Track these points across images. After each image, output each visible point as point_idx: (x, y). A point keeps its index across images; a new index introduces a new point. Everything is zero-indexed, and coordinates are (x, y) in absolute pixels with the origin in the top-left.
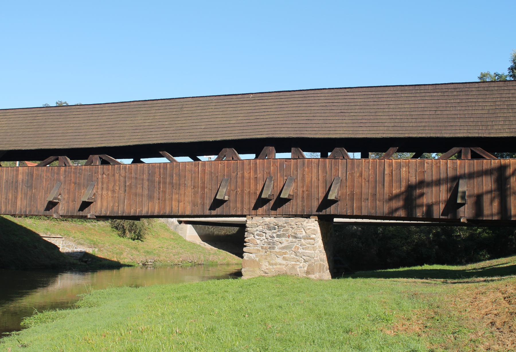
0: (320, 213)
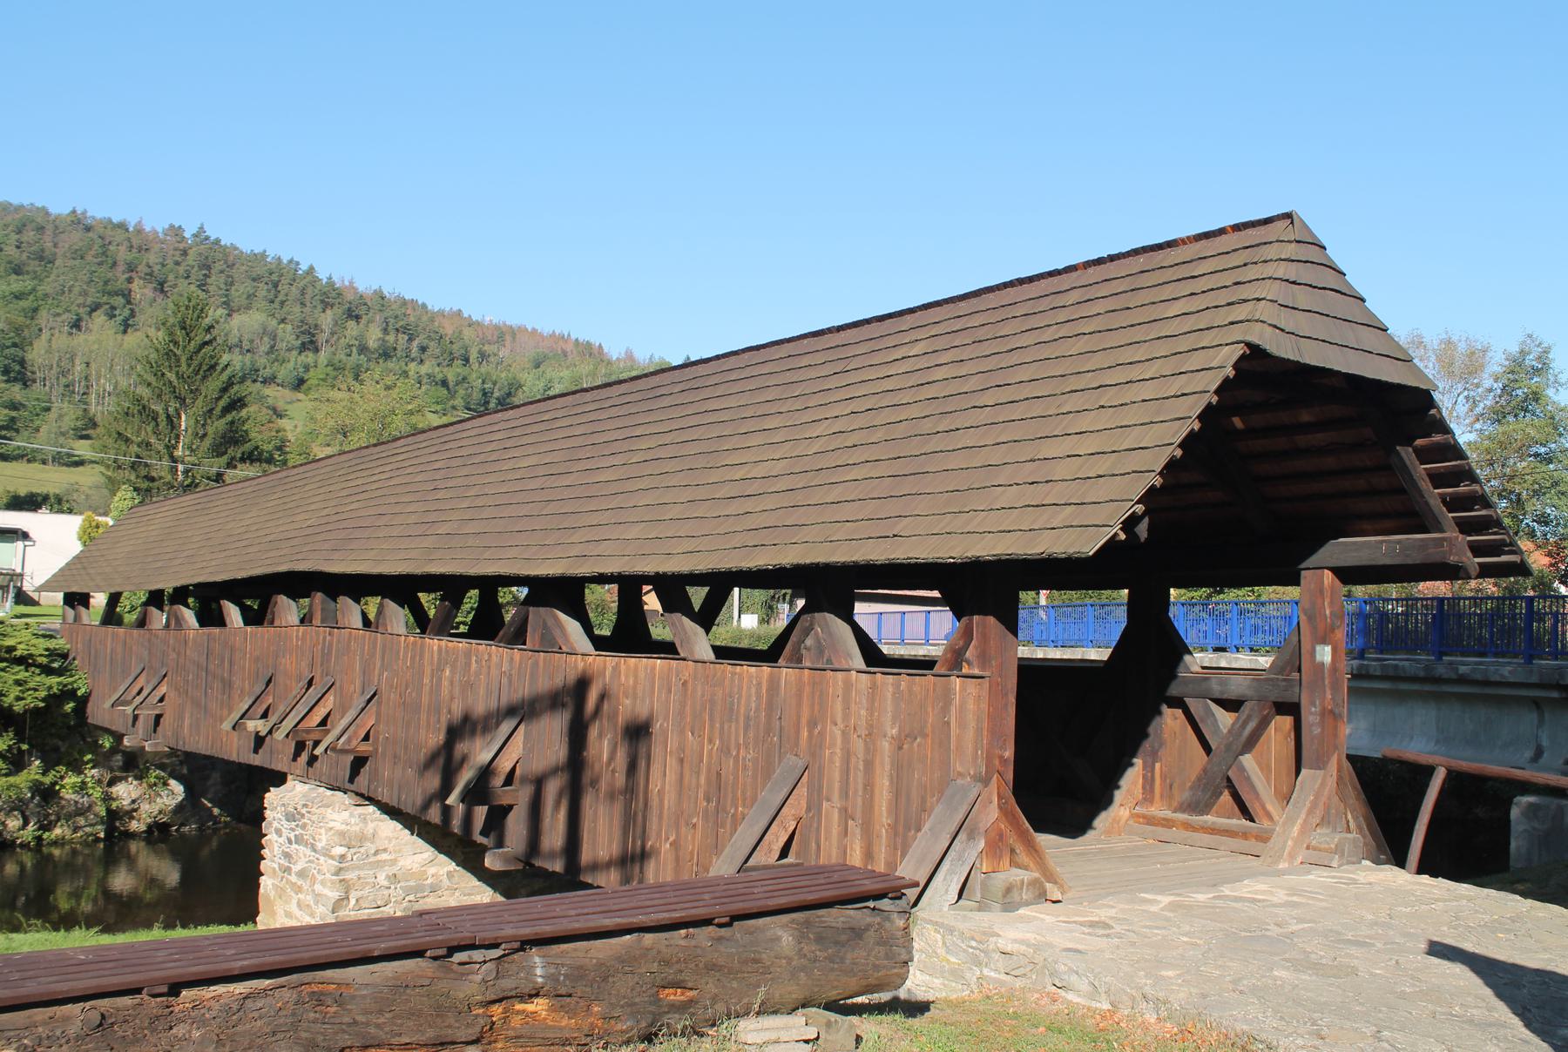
0: (353, 787)
